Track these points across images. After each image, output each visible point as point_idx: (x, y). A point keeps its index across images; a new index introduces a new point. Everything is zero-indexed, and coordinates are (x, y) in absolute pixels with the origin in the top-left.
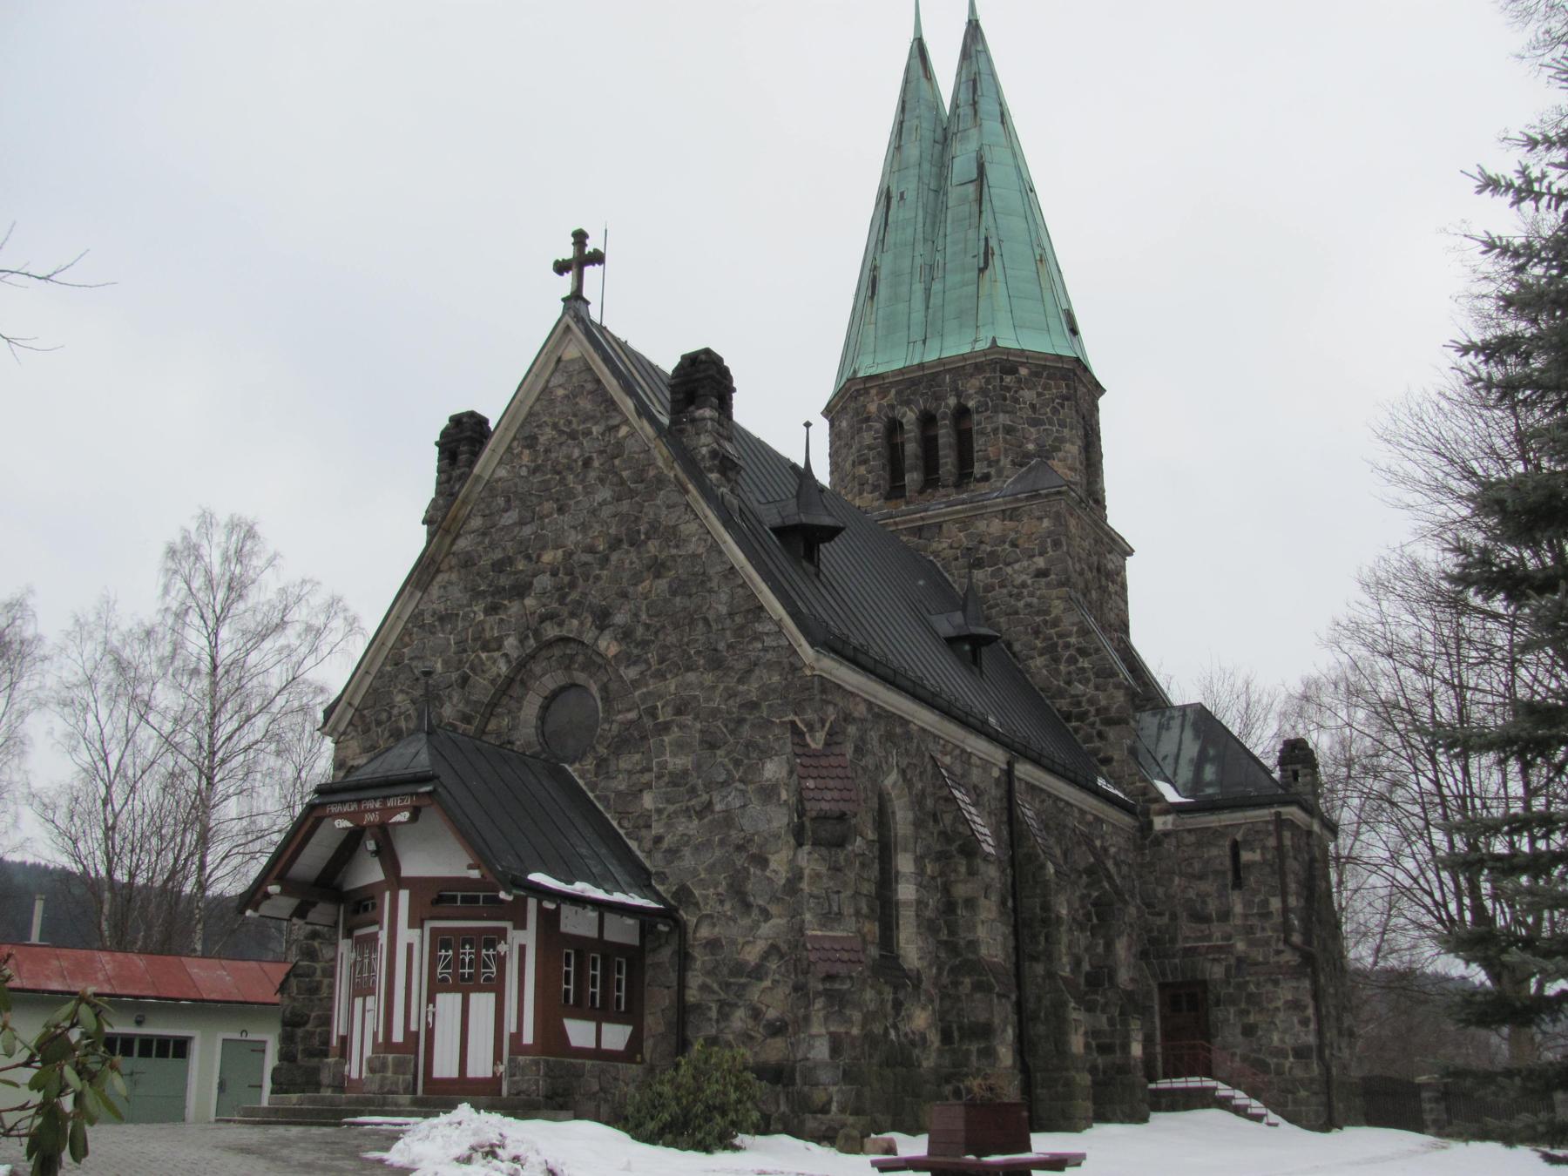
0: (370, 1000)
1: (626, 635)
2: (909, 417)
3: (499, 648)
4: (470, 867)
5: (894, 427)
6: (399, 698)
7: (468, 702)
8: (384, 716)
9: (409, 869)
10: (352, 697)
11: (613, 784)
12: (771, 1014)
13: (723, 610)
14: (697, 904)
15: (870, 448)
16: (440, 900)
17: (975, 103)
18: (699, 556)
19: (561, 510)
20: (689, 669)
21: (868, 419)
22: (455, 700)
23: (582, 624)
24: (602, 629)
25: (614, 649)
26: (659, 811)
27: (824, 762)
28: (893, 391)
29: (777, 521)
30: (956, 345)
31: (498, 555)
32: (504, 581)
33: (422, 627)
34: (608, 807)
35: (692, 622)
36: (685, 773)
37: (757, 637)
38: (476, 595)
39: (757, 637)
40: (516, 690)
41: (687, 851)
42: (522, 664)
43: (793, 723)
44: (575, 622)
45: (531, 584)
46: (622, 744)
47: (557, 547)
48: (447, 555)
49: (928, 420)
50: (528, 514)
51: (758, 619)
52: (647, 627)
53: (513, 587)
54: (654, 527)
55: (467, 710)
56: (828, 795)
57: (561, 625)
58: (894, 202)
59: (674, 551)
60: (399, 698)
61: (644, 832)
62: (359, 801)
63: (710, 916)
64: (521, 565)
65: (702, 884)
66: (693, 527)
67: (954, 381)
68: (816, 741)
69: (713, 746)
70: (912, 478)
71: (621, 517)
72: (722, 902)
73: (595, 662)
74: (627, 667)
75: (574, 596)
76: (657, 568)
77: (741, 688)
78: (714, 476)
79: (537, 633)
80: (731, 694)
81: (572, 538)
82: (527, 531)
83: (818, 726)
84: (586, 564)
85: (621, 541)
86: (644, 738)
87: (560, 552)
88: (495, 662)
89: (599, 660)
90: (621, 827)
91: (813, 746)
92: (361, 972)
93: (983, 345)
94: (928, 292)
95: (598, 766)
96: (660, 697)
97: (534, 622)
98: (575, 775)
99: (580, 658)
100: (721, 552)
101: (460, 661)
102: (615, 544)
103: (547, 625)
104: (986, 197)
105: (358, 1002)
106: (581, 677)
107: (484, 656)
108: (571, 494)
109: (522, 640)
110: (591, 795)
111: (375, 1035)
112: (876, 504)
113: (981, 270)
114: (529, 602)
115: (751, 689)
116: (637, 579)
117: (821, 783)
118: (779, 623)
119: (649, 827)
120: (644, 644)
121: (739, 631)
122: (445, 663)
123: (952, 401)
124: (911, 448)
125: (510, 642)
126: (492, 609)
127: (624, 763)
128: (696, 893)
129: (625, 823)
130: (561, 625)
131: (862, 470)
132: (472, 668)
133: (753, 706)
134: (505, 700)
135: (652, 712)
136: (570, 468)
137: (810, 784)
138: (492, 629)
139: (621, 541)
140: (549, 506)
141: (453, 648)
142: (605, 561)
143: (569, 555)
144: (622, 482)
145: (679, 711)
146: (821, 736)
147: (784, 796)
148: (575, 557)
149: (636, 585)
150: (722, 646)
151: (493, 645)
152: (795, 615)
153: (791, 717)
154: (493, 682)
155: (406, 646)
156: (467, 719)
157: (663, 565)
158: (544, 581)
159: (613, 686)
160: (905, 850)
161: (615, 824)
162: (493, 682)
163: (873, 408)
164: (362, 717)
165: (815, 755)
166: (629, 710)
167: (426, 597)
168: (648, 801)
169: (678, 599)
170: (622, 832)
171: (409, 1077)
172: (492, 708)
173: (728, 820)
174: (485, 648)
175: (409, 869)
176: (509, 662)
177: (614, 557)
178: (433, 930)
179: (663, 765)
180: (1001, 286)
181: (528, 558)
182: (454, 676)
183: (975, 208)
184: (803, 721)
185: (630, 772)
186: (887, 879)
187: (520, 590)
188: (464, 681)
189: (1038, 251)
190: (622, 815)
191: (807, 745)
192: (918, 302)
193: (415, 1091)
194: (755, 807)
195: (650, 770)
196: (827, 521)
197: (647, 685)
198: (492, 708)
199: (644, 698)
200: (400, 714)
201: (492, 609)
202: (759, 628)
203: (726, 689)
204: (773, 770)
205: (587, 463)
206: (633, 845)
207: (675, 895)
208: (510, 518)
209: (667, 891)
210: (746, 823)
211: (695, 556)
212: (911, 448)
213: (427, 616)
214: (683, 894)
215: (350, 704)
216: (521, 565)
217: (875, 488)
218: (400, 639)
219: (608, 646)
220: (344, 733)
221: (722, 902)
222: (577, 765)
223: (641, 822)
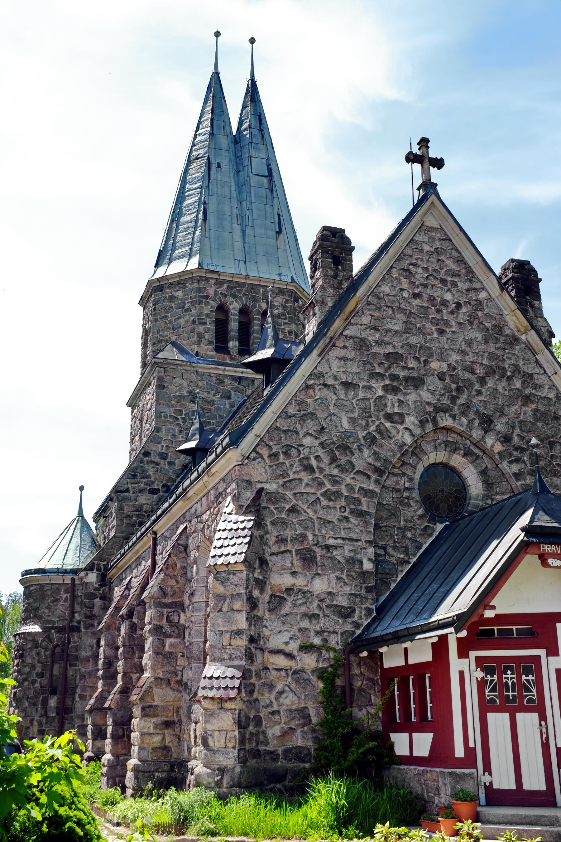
1: (506, 439)
2: (234, 306)
3: (402, 423)
5: (222, 309)
15: (207, 315)
17: (261, 130)
21: (207, 297)
24: (486, 431)
28: (225, 286)
49: (244, 311)
54: (517, 369)
55: (378, 464)
58: (214, 167)
70: (233, 345)
71: (492, 356)
94: (243, 231)
102: (490, 372)
104: (274, 189)
112: (211, 353)
113: (279, 232)
123: (264, 306)
124: (234, 326)
125: (411, 420)
126: (390, 389)
130: (454, 417)
131: (201, 328)
142: (482, 381)
158: (433, 382)
163: (211, 291)
183: (269, 193)
187: (417, 382)
197: (525, 479)
201: (390, 389)
205: (459, 306)
212: (234, 326)
217: (210, 343)
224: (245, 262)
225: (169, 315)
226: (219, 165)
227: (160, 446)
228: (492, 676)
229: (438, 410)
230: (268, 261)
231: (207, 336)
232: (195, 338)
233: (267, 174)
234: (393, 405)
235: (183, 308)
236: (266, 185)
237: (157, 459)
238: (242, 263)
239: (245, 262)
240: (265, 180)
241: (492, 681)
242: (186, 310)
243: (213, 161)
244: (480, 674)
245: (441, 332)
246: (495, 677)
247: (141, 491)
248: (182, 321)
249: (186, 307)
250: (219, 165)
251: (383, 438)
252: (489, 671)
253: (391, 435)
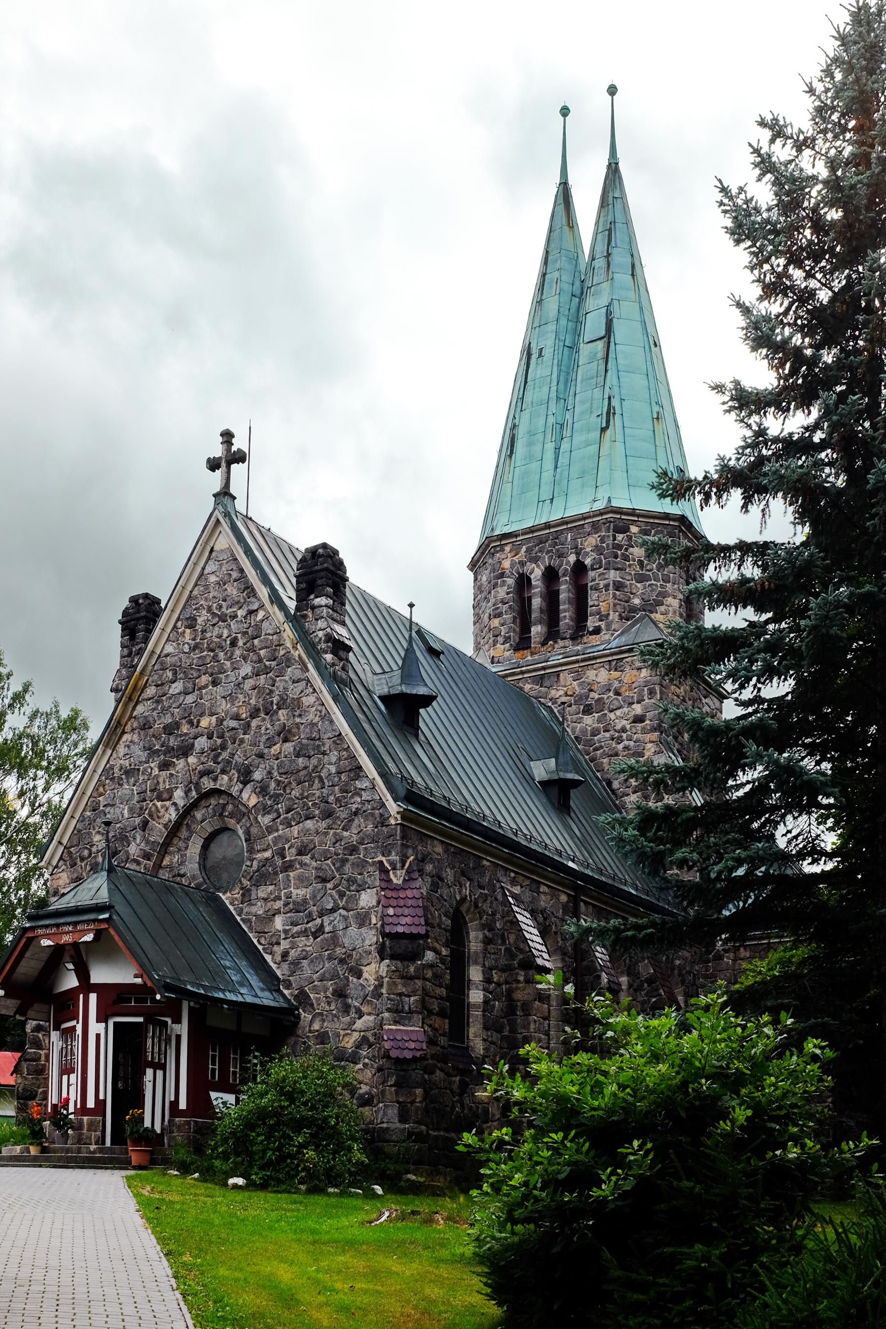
0: (73, 1077)
1: (262, 790)
4: (136, 976)
6: (97, 838)
7: (148, 842)
8: (86, 853)
9: (93, 980)
10: (61, 837)
11: (254, 909)
12: (364, 1089)
13: (333, 769)
14: (312, 1005)
16: (115, 1003)
18: (316, 724)
19: (215, 683)
20: (308, 818)
22: (138, 841)
23: (230, 780)
24: (245, 783)
25: (253, 801)
26: (286, 932)
27: (402, 894)
29: (385, 691)
30: (579, 504)
31: (168, 720)
32: (173, 742)
33: (112, 779)
34: (250, 928)
35: (311, 780)
36: (305, 901)
37: (358, 792)
38: (152, 753)
39: (358, 792)
40: (184, 833)
41: (305, 963)
42: (187, 813)
43: (381, 862)
44: (226, 778)
45: (193, 745)
46: (262, 877)
47: (212, 715)
48: (129, 719)
50: (190, 685)
51: (357, 777)
52: (278, 783)
53: (180, 748)
55: (147, 849)
56: (403, 921)
57: (215, 780)
59: (298, 720)
60: (97, 838)
61: (276, 948)
63: (321, 1014)
64: (185, 729)
65: (316, 990)
66: (312, 699)
67: (574, 539)
68: (397, 878)
69: (324, 880)
72: (329, 1004)
73: (242, 812)
74: (263, 815)
75: (225, 755)
76: (285, 734)
77: (345, 834)
78: (329, 657)
79: (197, 785)
80: (338, 840)
82: (190, 699)
83: (398, 865)
84: (233, 729)
85: (258, 710)
86: (276, 874)
87: (214, 719)
88: (167, 810)
89: (243, 809)
90: (260, 944)
91: (395, 881)
92: (66, 1056)
93: (600, 505)
95: (243, 895)
96: (288, 841)
97: (195, 779)
98: (227, 902)
99: (230, 807)
100: (332, 722)
101: (141, 809)
103: (205, 780)
105: (65, 1077)
106: (231, 823)
107: (159, 804)
108: (222, 671)
109: (187, 792)
110: (238, 918)
111: (76, 1102)
114: (192, 760)
115: (351, 836)
116: (270, 743)
117: (399, 911)
118: (372, 782)
119: (278, 944)
120: (276, 798)
121: (344, 791)
122: (131, 810)
125: (178, 794)
126: (165, 766)
127: (263, 892)
128: (312, 996)
129: (263, 941)
130: (215, 780)
132: (151, 815)
133: (353, 850)
134: (175, 841)
135: (282, 854)
136: (221, 647)
137: (391, 911)
138: (164, 782)
139: (258, 710)
140: (205, 679)
141: (136, 798)
142: (247, 728)
143: (220, 721)
144: (260, 660)
145: (300, 853)
146: (401, 873)
147: (374, 921)
148: (225, 723)
149: (269, 747)
150: (331, 799)
151: (165, 796)
152: (385, 775)
153: (380, 858)
154: (166, 826)
155: (101, 795)
156: (147, 856)
157: (289, 731)
159: (254, 830)
160: (476, 963)
161: (255, 941)
162: (166, 826)
164: (70, 853)
165: (397, 889)
166: (265, 850)
167: (114, 755)
168: (279, 923)
169: (301, 760)
170: (260, 948)
171: (99, 1133)
172: (165, 847)
173: (334, 940)
174: (160, 798)
175: (93, 980)
176: (177, 809)
177: (254, 723)
178: (115, 1023)
179: (289, 896)
180: (619, 446)
181: (191, 723)
182: (138, 820)
184: (388, 861)
185: (265, 899)
186: (460, 984)
187: (185, 751)
188: (145, 825)
189: (656, 409)
190: (261, 933)
191: (390, 881)
192: (549, 464)
193: (104, 1143)
194: (353, 930)
195: (280, 899)
196: (422, 691)
198: (165, 847)
199: (276, 840)
200: (98, 851)
202: (358, 784)
203: (335, 834)
204: (367, 899)
206: (268, 958)
207: (296, 997)
208: (177, 687)
209: (291, 994)
210: (346, 941)
211: (313, 725)
213: (116, 770)
214: (303, 998)
215: (60, 843)
216: (185, 729)
218: (96, 789)
219: (249, 798)
220: (56, 867)
221: (329, 1004)
222: (228, 894)
223: (274, 940)
229: (203, 774)
234: (164, 782)
253: (160, 815)
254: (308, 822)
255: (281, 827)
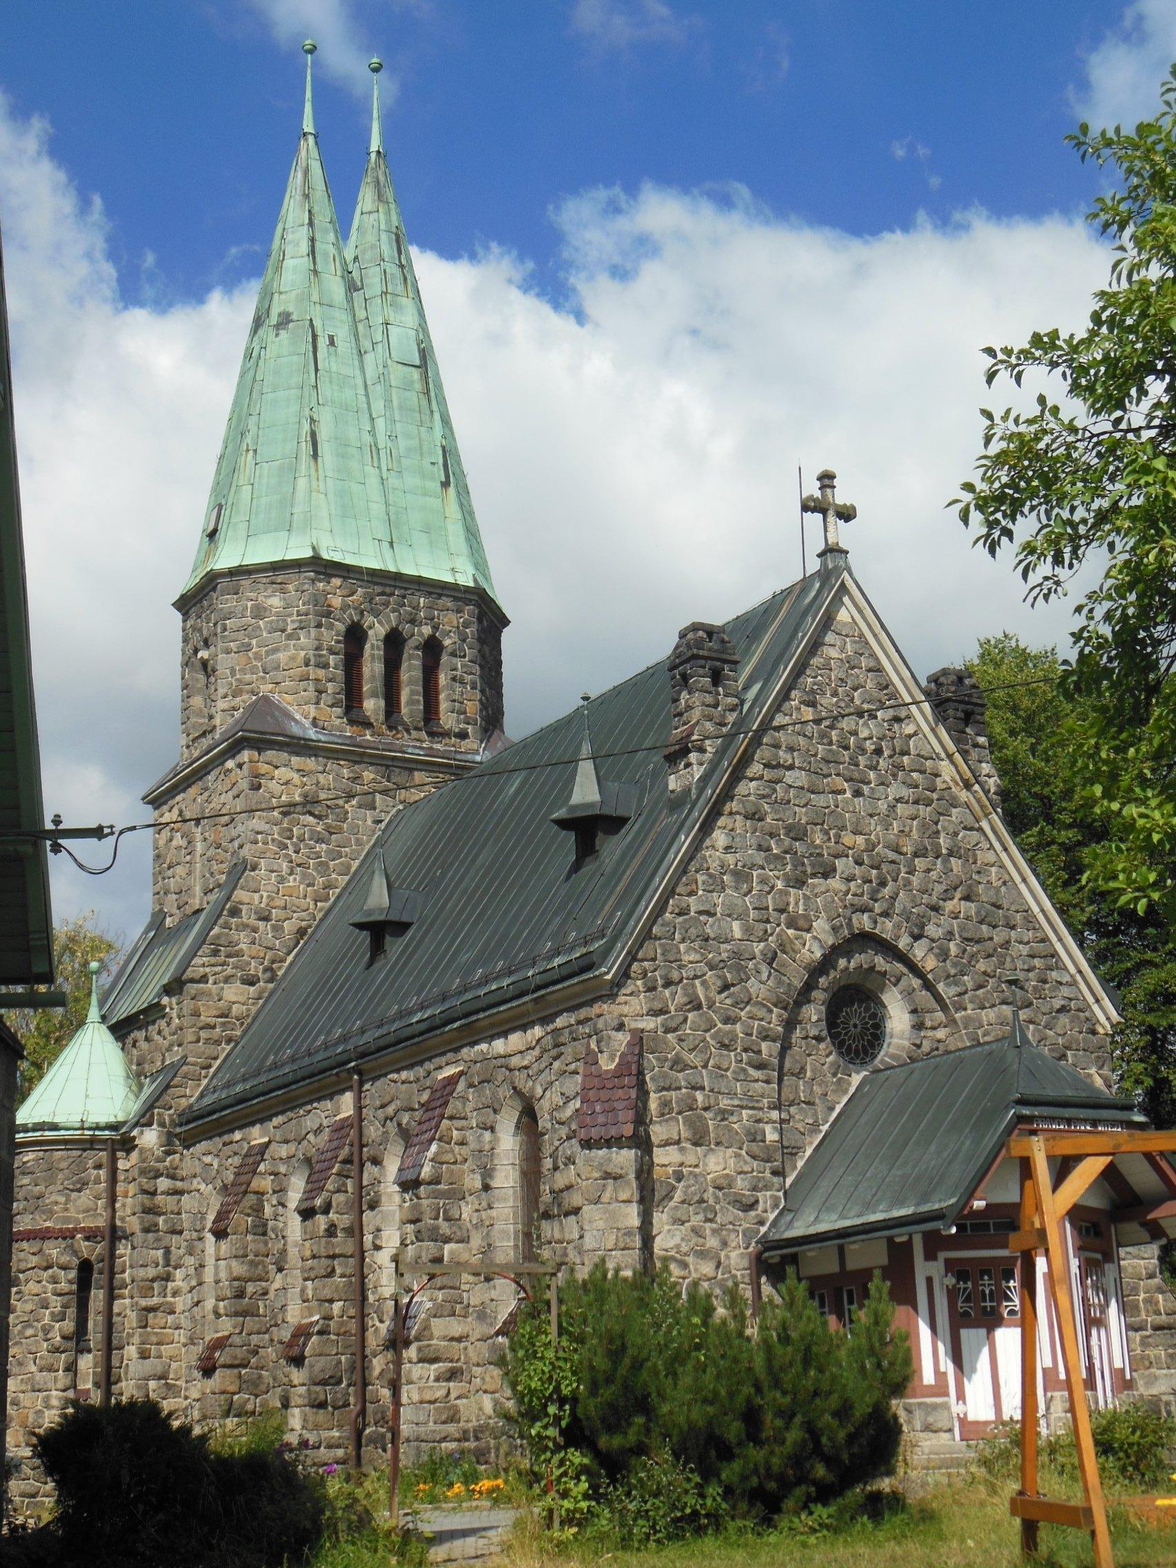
2: (377, 630)
5: (355, 636)
24: (916, 938)
49: (394, 642)
58: (322, 342)
62: (1095, 1123)
81: (875, 828)
123: (427, 630)
125: (821, 925)
183: (424, 402)
224: (391, 544)
225: (254, 642)
226: (331, 338)
227: (256, 896)
228: (965, 1283)
230: (431, 543)
231: (330, 687)
232: (311, 694)
233: (417, 362)
235: (283, 631)
236: (418, 386)
237: (253, 921)
238: (386, 545)
239: (391, 544)
240: (416, 374)
241: (965, 1289)
242: (289, 637)
243: (319, 332)
244: (950, 1281)
245: (858, 793)
246: (970, 1284)
247: (227, 980)
248: (282, 656)
249: (289, 631)
250: (331, 338)
251: (785, 953)
252: (962, 1276)
254: (1004, 1007)
255: (970, 1006)
